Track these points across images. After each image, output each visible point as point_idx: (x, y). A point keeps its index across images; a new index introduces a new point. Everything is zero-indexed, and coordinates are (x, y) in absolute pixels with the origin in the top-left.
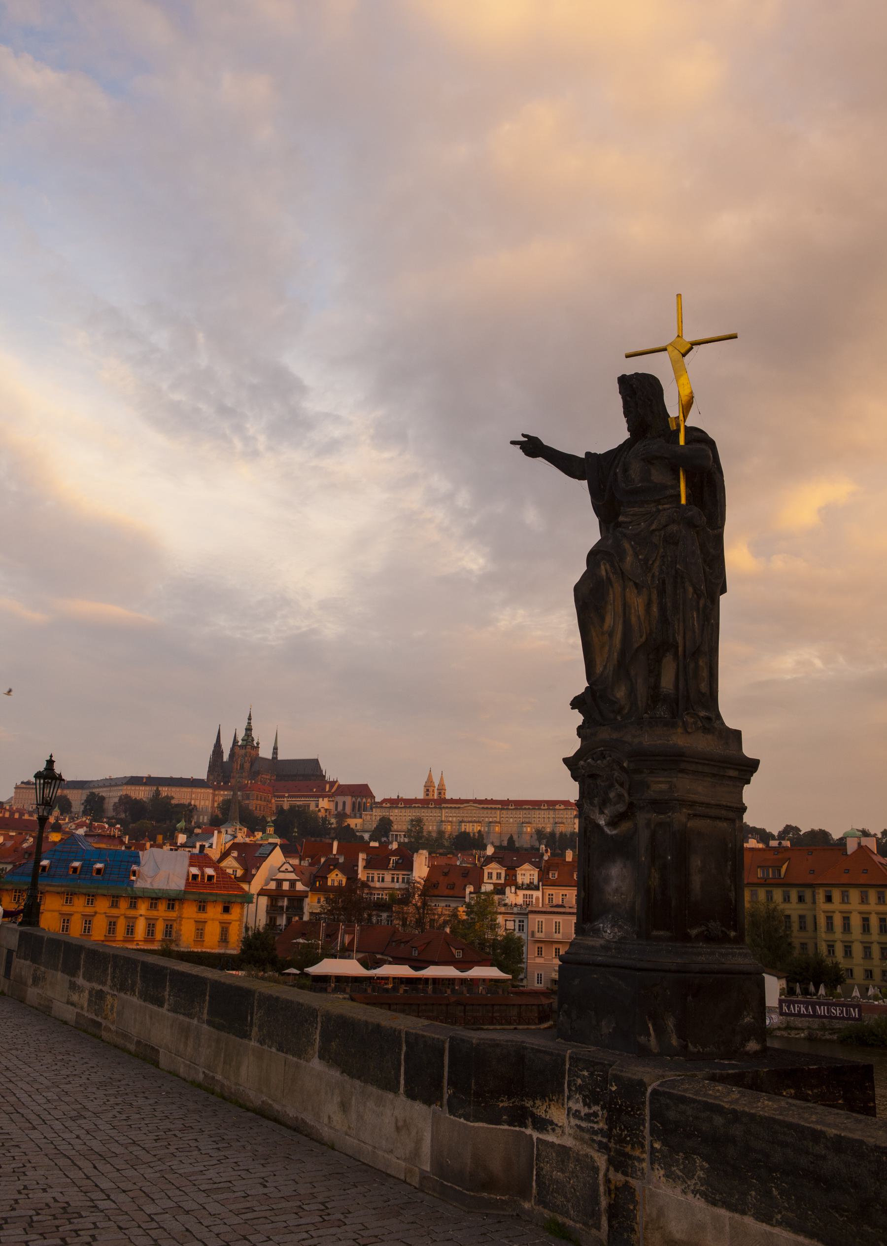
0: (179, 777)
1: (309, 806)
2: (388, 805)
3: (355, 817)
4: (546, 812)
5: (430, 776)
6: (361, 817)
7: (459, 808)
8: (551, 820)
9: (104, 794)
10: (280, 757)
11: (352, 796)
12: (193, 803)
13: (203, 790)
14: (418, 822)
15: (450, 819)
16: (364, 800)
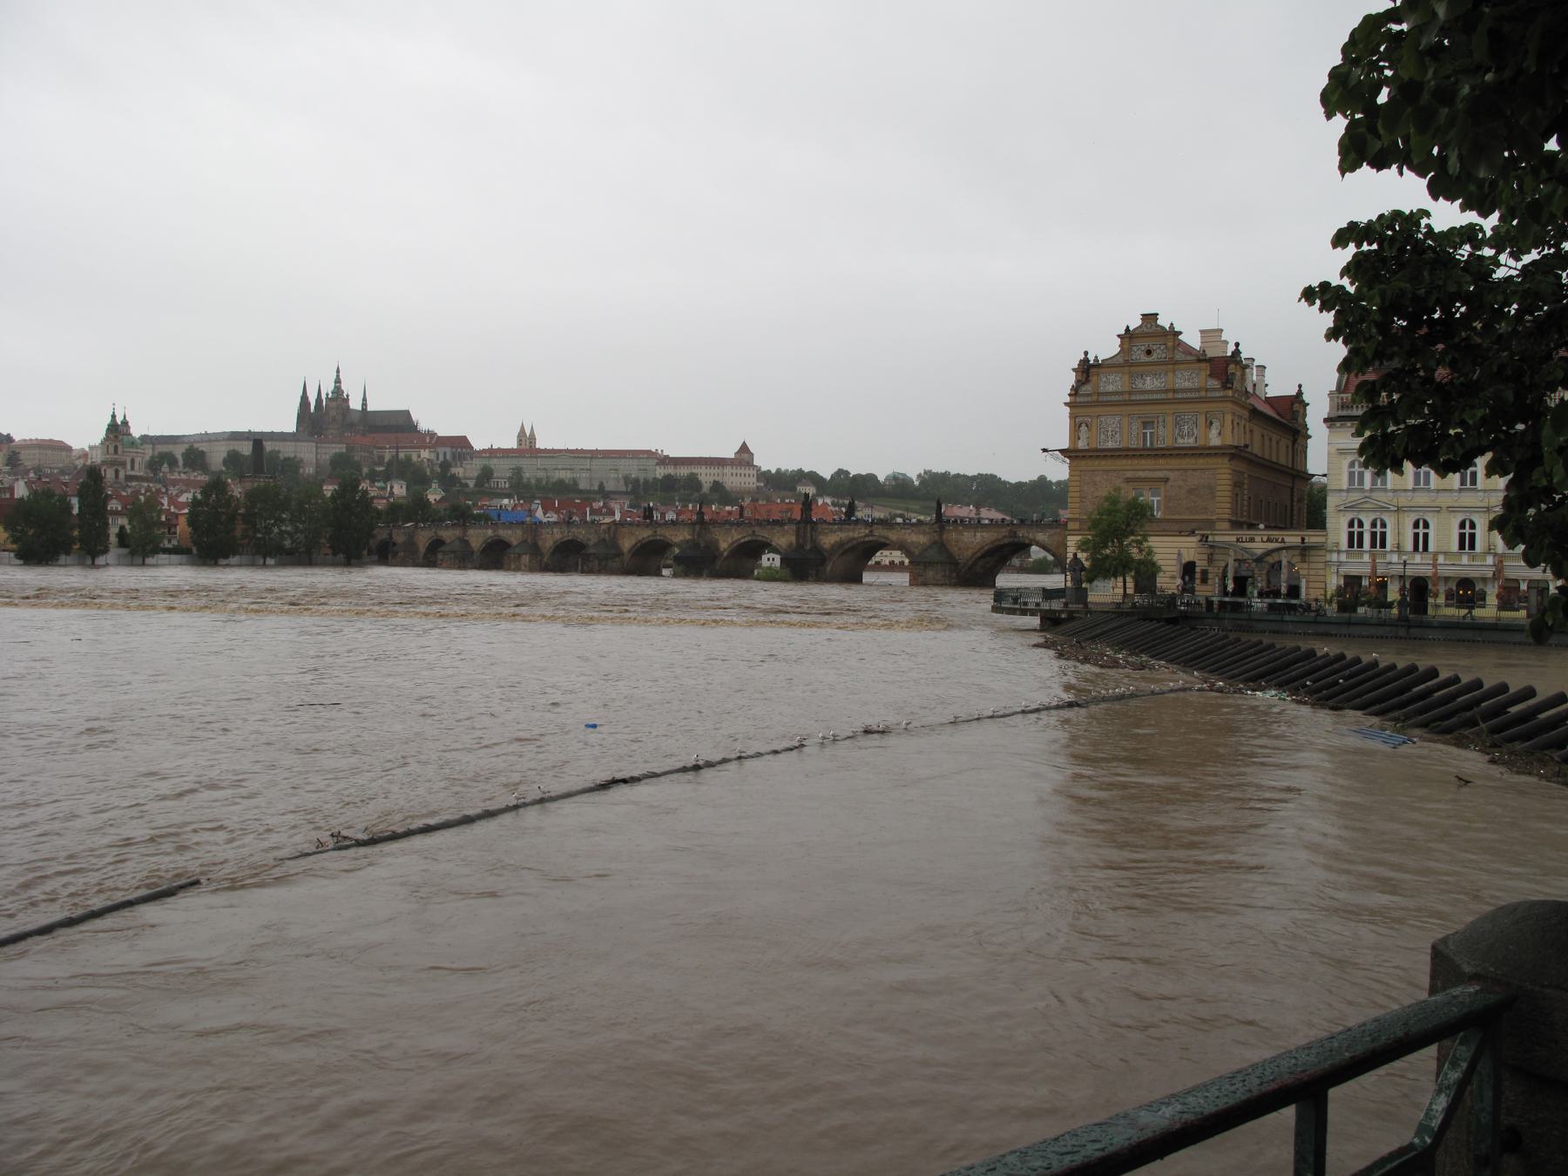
0: (279, 431)
1: (410, 456)
2: (488, 455)
3: (456, 466)
4: (631, 460)
5: (522, 427)
6: (461, 466)
7: (553, 457)
8: (635, 467)
9: (204, 449)
10: (370, 408)
11: (452, 447)
12: (298, 455)
13: (305, 444)
14: (518, 471)
15: (547, 467)
16: (464, 450)
